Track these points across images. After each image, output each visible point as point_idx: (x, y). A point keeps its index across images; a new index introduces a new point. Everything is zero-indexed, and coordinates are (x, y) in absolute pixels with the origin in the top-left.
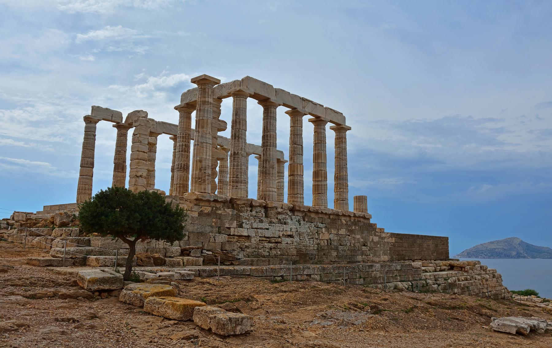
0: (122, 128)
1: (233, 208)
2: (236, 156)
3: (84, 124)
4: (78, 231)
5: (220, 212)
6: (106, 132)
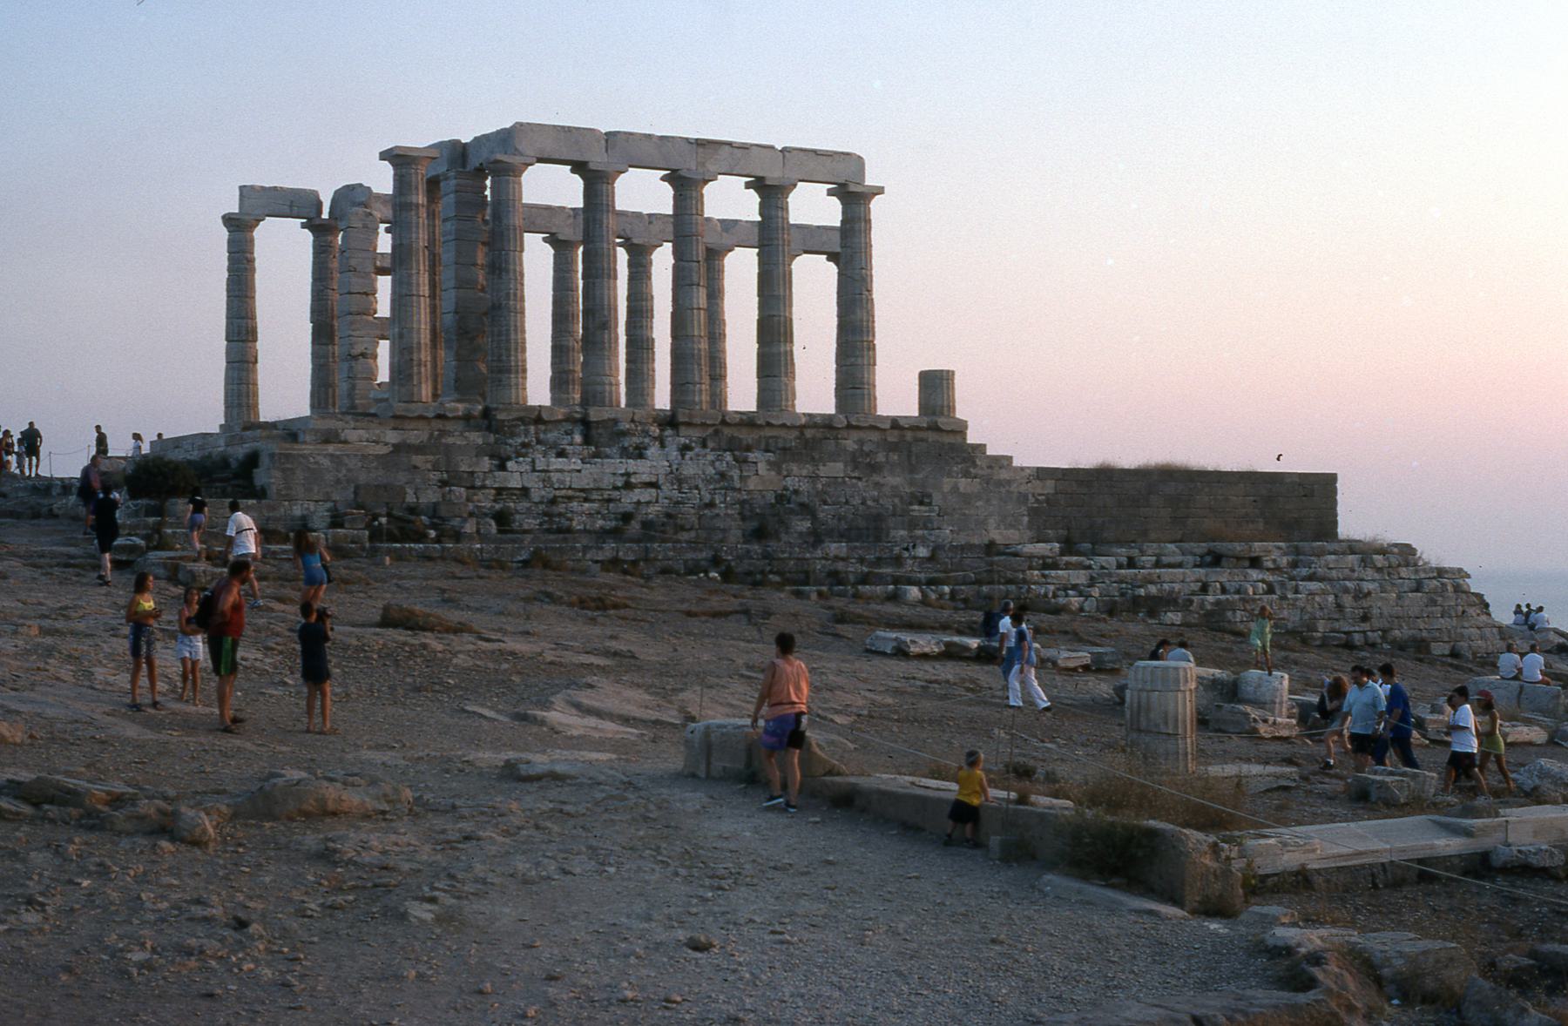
1: (489, 429)
5: (450, 440)
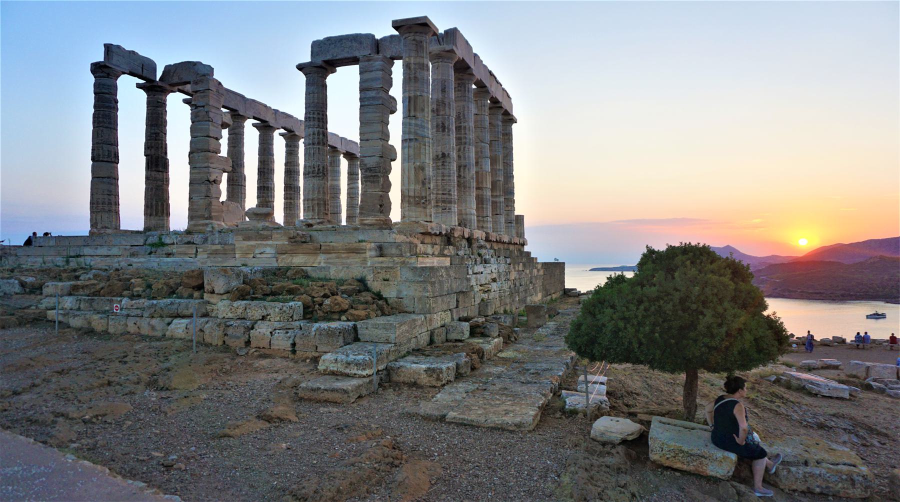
0: (155, 91)
2: (448, 160)
3: (92, 79)
4: (302, 307)
6: (131, 97)
